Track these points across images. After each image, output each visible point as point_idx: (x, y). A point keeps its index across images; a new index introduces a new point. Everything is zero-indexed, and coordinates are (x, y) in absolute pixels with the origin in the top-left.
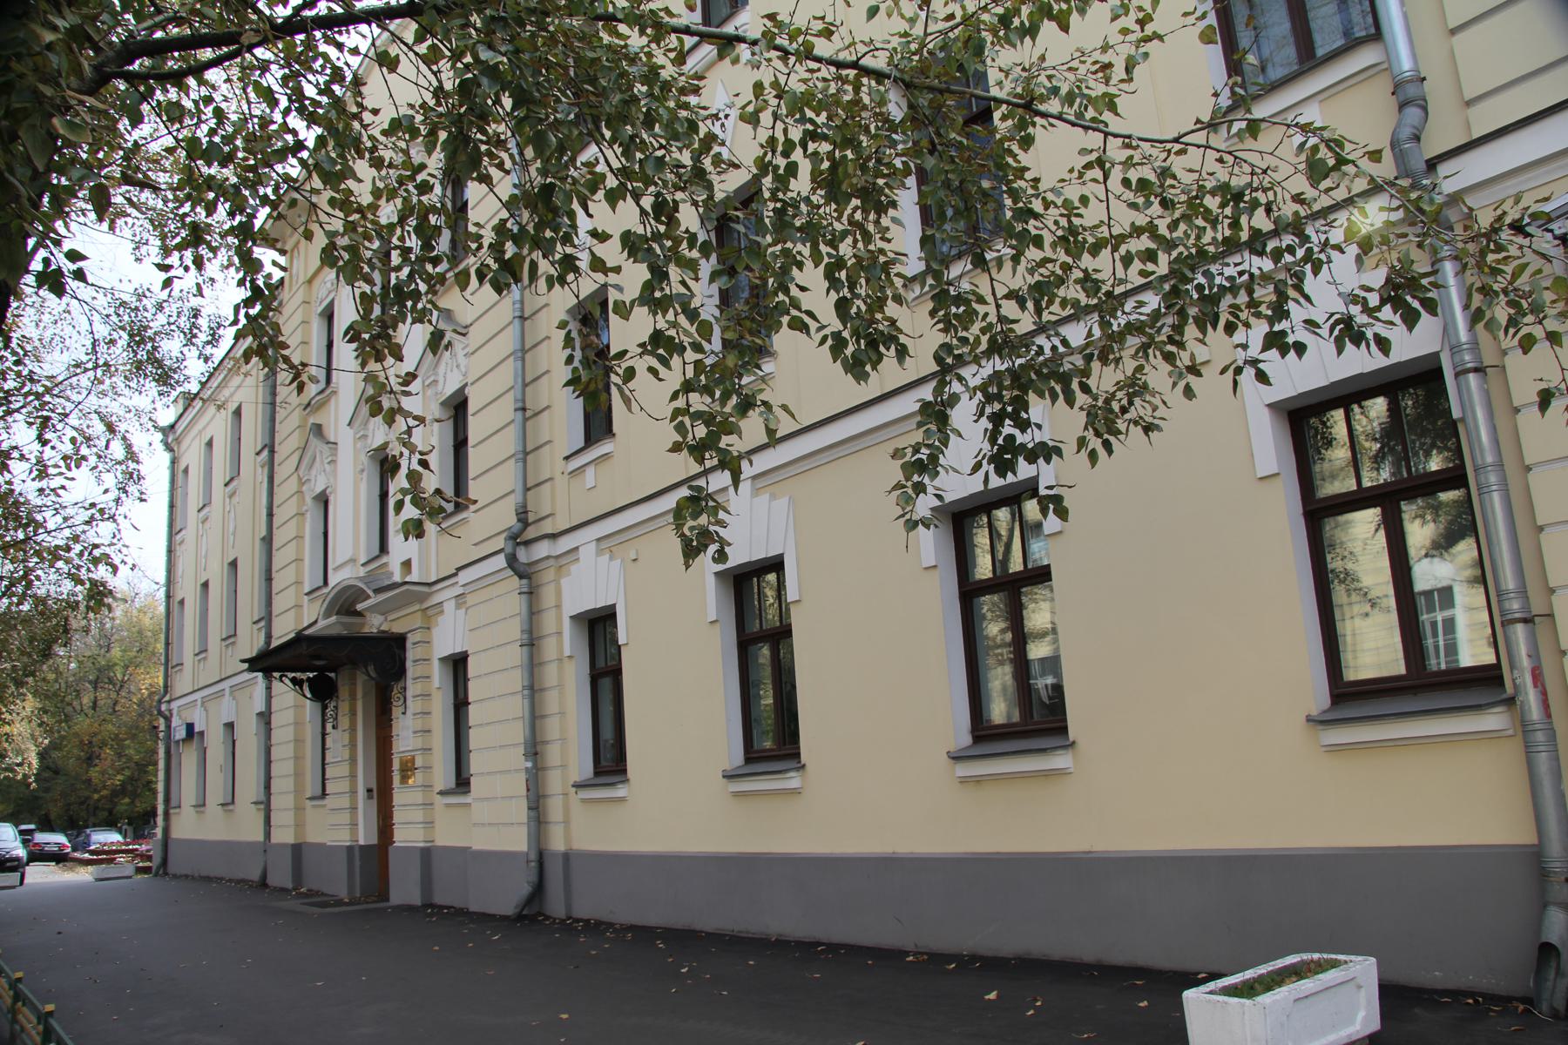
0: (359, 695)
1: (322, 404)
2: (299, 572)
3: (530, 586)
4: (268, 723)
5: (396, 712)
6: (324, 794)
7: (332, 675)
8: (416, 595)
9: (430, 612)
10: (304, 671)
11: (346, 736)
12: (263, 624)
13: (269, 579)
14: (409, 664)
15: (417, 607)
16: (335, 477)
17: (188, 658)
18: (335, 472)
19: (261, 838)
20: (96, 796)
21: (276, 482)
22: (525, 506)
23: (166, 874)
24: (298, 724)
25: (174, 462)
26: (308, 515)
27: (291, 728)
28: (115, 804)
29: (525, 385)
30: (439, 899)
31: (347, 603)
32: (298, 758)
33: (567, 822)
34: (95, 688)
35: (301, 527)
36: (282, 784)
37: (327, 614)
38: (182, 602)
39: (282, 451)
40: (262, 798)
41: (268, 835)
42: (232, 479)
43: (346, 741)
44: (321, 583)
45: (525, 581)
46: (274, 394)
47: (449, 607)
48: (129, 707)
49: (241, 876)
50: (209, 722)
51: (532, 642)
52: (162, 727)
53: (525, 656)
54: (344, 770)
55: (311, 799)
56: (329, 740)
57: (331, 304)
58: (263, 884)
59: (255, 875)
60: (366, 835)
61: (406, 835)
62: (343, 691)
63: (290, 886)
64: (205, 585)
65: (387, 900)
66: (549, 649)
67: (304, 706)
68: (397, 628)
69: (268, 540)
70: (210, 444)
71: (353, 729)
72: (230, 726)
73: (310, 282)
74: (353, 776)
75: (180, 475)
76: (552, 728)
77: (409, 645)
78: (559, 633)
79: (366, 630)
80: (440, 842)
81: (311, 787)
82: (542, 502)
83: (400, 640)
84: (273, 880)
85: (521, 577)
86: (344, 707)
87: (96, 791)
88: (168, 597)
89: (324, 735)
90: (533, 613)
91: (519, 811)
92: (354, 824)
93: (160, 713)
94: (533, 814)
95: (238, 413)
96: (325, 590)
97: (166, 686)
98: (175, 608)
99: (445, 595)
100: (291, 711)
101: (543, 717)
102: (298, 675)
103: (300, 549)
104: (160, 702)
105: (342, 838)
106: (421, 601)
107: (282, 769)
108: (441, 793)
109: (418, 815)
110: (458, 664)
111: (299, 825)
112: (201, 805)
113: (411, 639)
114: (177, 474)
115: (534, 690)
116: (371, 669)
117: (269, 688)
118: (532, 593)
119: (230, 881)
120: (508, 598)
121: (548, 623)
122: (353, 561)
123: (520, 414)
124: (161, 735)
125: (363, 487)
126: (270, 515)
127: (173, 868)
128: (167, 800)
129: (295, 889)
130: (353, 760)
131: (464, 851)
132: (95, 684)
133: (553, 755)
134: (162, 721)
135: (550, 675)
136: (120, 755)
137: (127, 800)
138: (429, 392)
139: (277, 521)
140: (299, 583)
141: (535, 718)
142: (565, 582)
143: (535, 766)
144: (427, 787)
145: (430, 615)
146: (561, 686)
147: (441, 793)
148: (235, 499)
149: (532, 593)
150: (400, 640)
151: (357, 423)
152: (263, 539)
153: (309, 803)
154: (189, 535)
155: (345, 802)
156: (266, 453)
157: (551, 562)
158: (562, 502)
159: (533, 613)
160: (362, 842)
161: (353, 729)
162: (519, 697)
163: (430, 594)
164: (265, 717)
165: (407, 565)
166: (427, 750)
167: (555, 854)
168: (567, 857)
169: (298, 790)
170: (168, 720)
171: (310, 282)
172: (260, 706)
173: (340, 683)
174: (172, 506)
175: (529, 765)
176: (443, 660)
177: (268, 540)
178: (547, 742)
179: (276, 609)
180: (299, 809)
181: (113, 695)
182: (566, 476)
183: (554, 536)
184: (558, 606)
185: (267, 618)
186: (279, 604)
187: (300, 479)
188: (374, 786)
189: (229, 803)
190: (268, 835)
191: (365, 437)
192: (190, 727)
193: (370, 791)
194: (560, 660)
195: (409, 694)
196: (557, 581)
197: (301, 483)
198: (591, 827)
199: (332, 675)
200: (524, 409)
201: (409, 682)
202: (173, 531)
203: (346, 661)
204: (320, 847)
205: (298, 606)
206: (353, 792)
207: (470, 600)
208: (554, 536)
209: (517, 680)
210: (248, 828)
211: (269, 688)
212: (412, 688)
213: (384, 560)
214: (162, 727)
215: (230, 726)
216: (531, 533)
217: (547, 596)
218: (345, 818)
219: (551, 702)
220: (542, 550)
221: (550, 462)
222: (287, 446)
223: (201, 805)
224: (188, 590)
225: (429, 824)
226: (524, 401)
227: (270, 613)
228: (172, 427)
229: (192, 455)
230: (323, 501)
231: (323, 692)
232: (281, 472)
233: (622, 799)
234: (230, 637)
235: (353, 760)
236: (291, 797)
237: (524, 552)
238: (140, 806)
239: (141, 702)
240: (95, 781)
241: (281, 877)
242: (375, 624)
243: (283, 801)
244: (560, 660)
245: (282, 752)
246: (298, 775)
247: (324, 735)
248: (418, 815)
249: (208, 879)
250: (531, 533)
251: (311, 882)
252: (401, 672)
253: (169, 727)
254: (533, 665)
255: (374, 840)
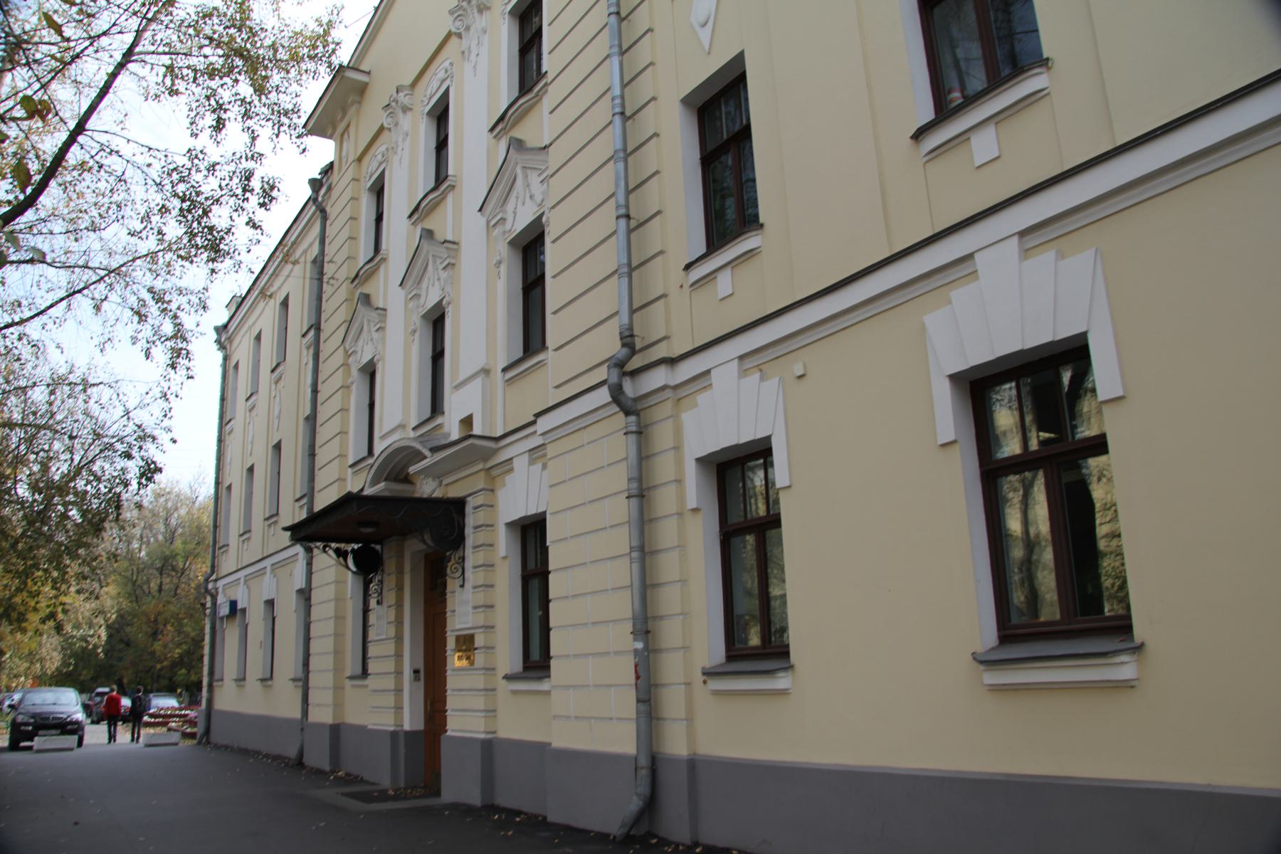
0: (407, 568)
1: (372, 274)
2: (344, 445)
3: (638, 424)
4: (308, 599)
5: (452, 584)
6: (365, 673)
7: (378, 547)
8: (477, 450)
9: (494, 472)
10: (348, 541)
11: (392, 613)
12: (305, 500)
13: (312, 455)
14: (469, 531)
15: (480, 466)
16: (384, 343)
17: (233, 539)
18: (383, 339)
19: (297, 714)
20: (159, 666)
21: (321, 360)
22: (631, 328)
23: (208, 742)
24: (339, 600)
25: (226, 359)
26: (354, 387)
27: (332, 604)
28: (175, 674)
29: (628, 192)
30: (503, 800)
31: (398, 466)
32: (338, 635)
33: (690, 719)
34: (161, 574)
35: (346, 399)
36: (321, 662)
37: (375, 481)
38: (229, 488)
39: (327, 328)
40: (300, 674)
41: (305, 712)
42: (278, 365)
43: (392, 618)
44: (365, 453)
45: (633, 418)
46: (321, 273)
47: (521, 464)
48: (188, 589)
49: (276, 750)
50: (251, 598)
51: (641, 493)
52: (209, 605)
53: (635, 513)
54: (390, 648)
55: (352, 678)
56: (372, 618)
57: (382, 175)
58: (299, 763)
59: (292, 752)
60: (411, 720)
61: (463, 721)
62: (390, 564)
63: (327, 768)
64: (251, 470)
65: (438, 793)
66: (665, 501)
67: (345, 582)
68: (454, 492)
69: (312, 419)
70: (258, 338)
71: (399, 605)
72: (270, 603)
73: (360, 160)
74: (399, 655)
75: (231, 371)
76: (669, 600)
77: (469, 509)
78: (679, 481)
79: (417, 495)
80: (503, 733)
81: (351, 664)
82: (653, 325)
83: (458, 505)
84: (310, 760)
85: (627, 413)
86: (390, 581)
87: (160, 662)
88: (218, 483)
89: (366, 611)
90: (644, 458)
91: (626, 703)
92: (399, 708)
93: (207, 590)
94: (643, 707)
95: (285, 304)
96: (371, 461)
97: (213, 566)
98: (224, 492)
99: (516, 450)
100: (333, 587)
101: (654, 586)
102: (342, 546)
103: (345, 422)
104: (207, 581)
105: (383, 721)
106: (486, 460)
107: (322, 646)
108: (507, 677)
109: (479, 702)
110: (532, 532)
111: (338, 705)
112: (241, 679)
113: (471, 503)
114: (229, 370)
115: (644, 552)
116: (427, 537)
117: (310, 564)
118: (641, 433)
119: (267, 756)
120: (611, 443)
121: (663, 469)
122: (401, 426)
123: (623, 222)
124: (208, 611)
125: (415, 349)
126: (315, 391)
127: (216, 737)
128: (211, 673)
129: (332, 772)
130: (399, 638)
131: (541, 749)
132: (161, 571)
133: (670, 633)
134: (209, 598)
135: (667, 533)
136: (180, 632)
137: (183, 671)
138: (497, 231)
139: (321, 398)
140: (342, 456)
141: (646, 587)
142: (687, 418)
143: (646, 648)
144: (490, 670)
145: (497, 472)
146: (681, 547)
147: (507, 677)
148: (281, 384)
149: (641, 433)
150: (458, 505)
151: (409, 283)
152: (307, 419)
153: (348, 683)
154: (237, 424)
155: (390, 683)
156: (312, 333)
157: (668, 393)
158: (679, 320)
159: (644, 458)
160: (407, 727)
161: (399, 605)
162: (627, 560)
163: (496, 451)
164: (305, 595)
165: (467, 422)
166: (489, 628)
167: (674, 761)
168: (693, 764)
169: (338, 669)
170: (214, 598)
171: (360, 160)
172: (300, 582)
173: (385, 556)
174: (223, 399)
175: (640, 645)
176: (510, 525)
177: (312, 419)
178: (661, 618)
179: (318, 486)
180: (338, 689)
181: (175, 580)
182: (686, 289)
183: (672, 362)
184: (677, 448)
185: (310, 494)
186: (322, 479)
187: (346, 351)
188: (421, 666)
189: (267, 679)
190: (305, 712)
191: (417, 296)
192: (233, 604)
193: (416, 672)
194: (680, 514)
195: (469, 564)
196: (676, 416)
197: (348, 355)
198: (721, 725)
199: (378, 547)
200: (628, 217)
201: (469, 551)
202: (224, 421)
203: (394, 530)
204: (361, 729)
205: (341, 480)
206: (399, 673)
207: (551, 451)
208: (672, 362)
209: (622, 540)
210: (285, 705)
211: (310, 564)
212: (472, 558)
213: (439, 420)
214: (209, 605)
215: (270, 603)
216: (636, 363)
217: (662, 436)
218: (390, 700)
219: (668, 567)
220: (659, 377)
221: (666, 276)
222: (333, 321)
223: (241, 679)
224: (235, 476)
225: (491, 712)
226: (627, 207)
227: (312, 489)
228: (225, 326)
229: (242, 351)
230: (370, 372)
231: (368, 565)
232: (326, 349)
233: (783, 692)
234: (273, 517)
235: (399, 638)
236: (331, 675)
237: (633, 384)
238: (194, 678)
239: (198, 586)
240: (158, 654)
241: (318, 757)
242: (427, 488)
243: (321, 679)
244: (680, 514)
245: (322, 628)
246: (338, 653)
247: (366, 611)
248: (479, 702)
249: (245, 752)
250: (636, 363)
251: (350, 765)
252: (458, 540)
253: (214, 603)
254: (644, 521)
255: (420, 726)
